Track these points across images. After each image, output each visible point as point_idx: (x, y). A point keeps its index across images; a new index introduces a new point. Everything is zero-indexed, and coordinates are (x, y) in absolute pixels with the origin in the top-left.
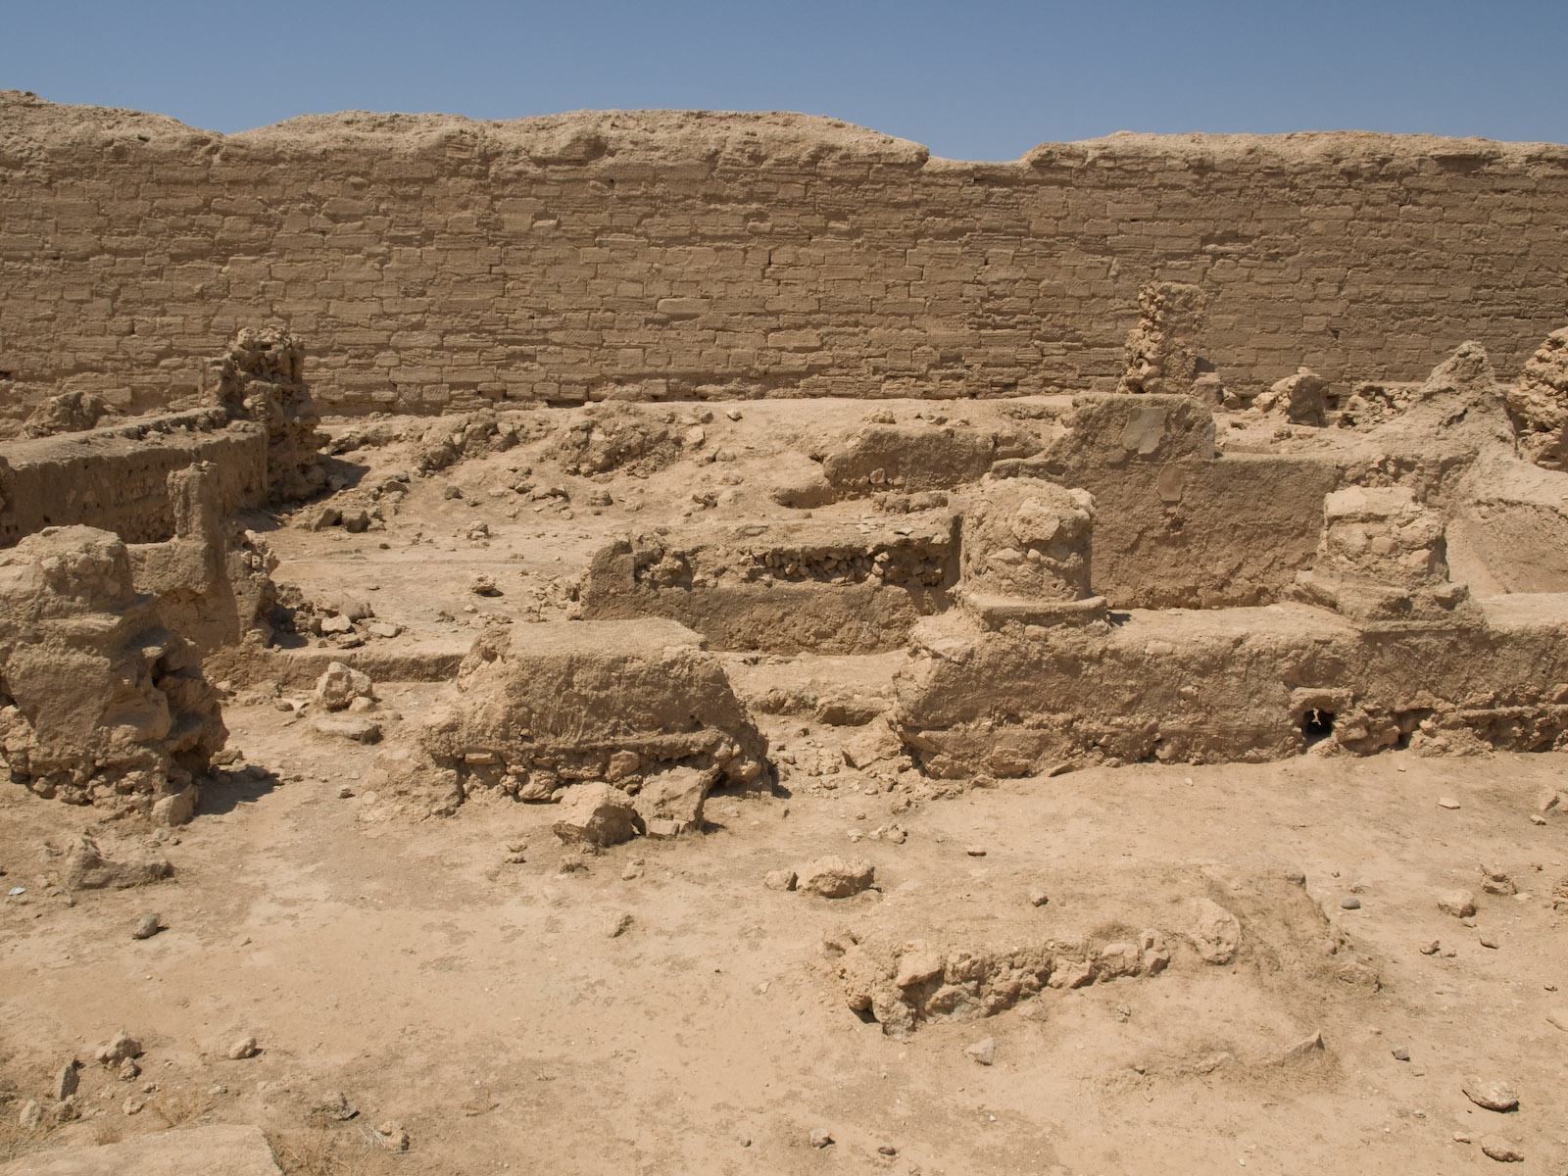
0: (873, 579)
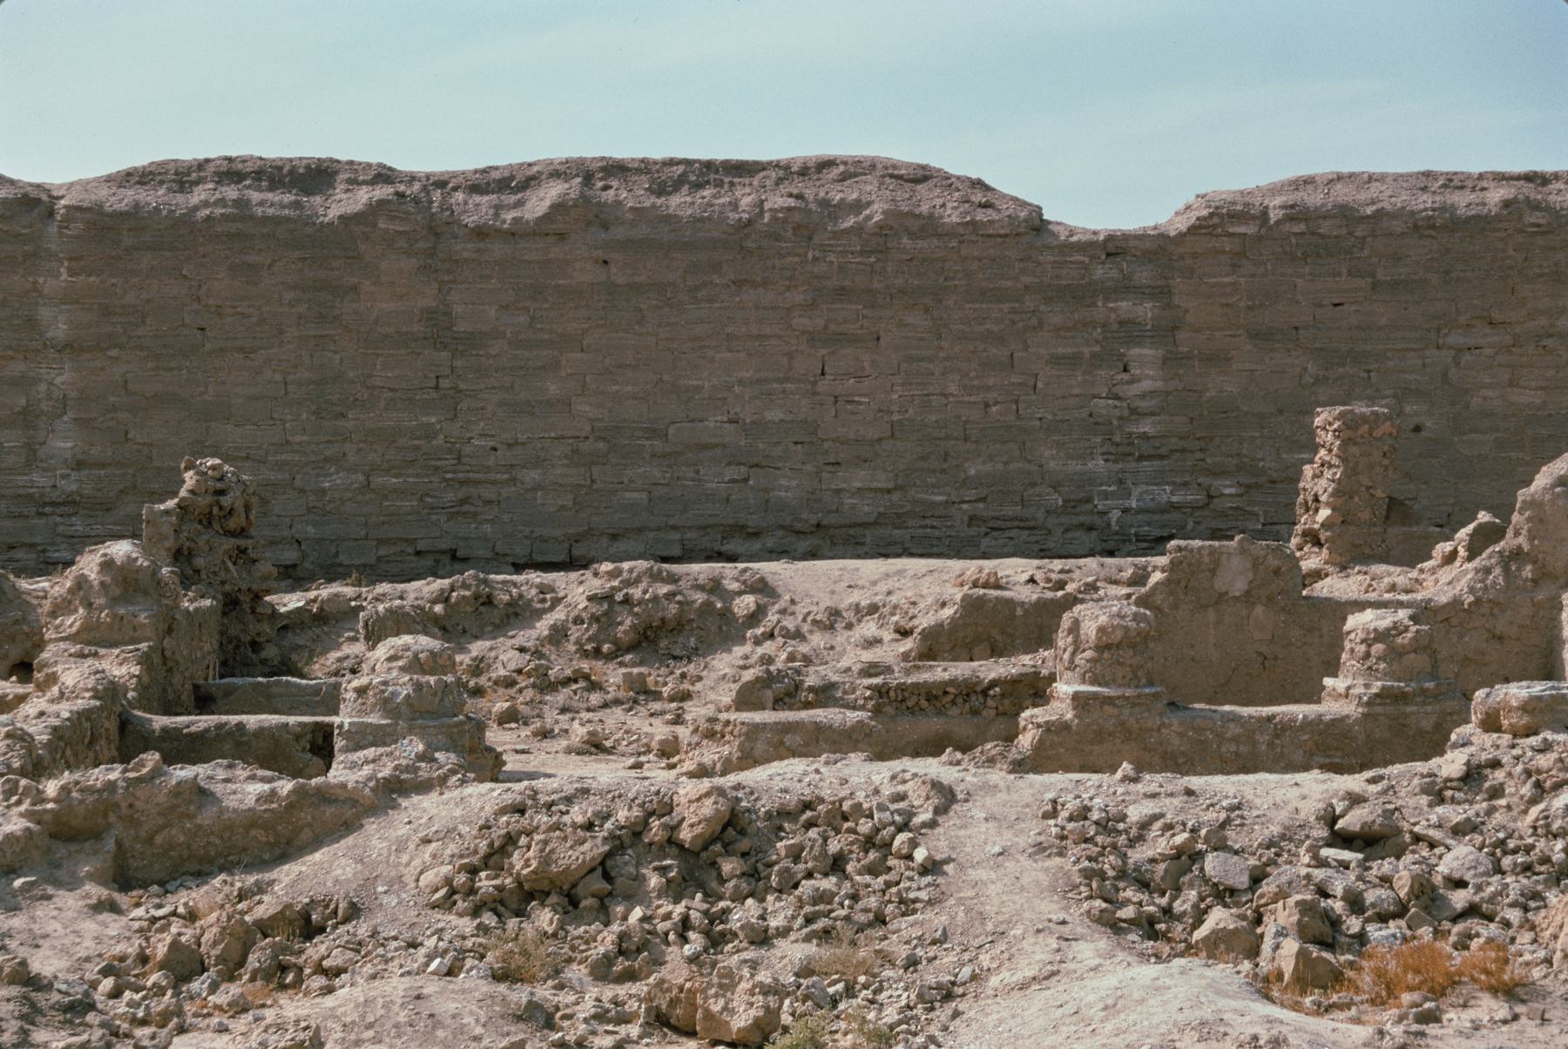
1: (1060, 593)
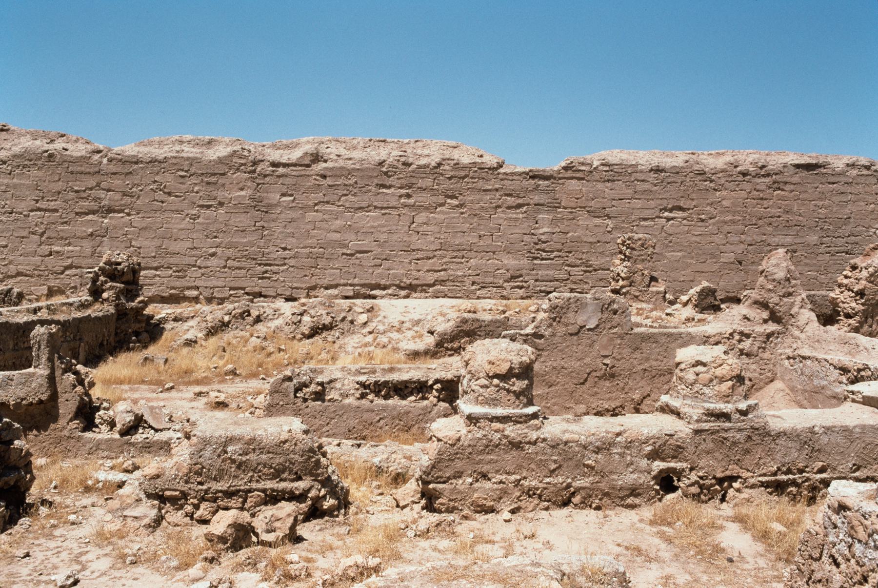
0: (432, 399)
1: (503, 316)
